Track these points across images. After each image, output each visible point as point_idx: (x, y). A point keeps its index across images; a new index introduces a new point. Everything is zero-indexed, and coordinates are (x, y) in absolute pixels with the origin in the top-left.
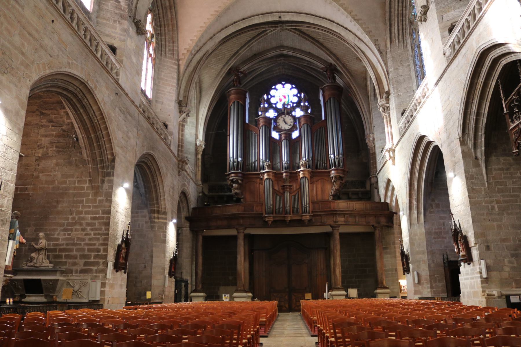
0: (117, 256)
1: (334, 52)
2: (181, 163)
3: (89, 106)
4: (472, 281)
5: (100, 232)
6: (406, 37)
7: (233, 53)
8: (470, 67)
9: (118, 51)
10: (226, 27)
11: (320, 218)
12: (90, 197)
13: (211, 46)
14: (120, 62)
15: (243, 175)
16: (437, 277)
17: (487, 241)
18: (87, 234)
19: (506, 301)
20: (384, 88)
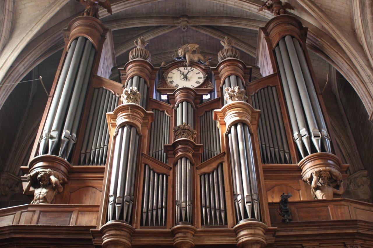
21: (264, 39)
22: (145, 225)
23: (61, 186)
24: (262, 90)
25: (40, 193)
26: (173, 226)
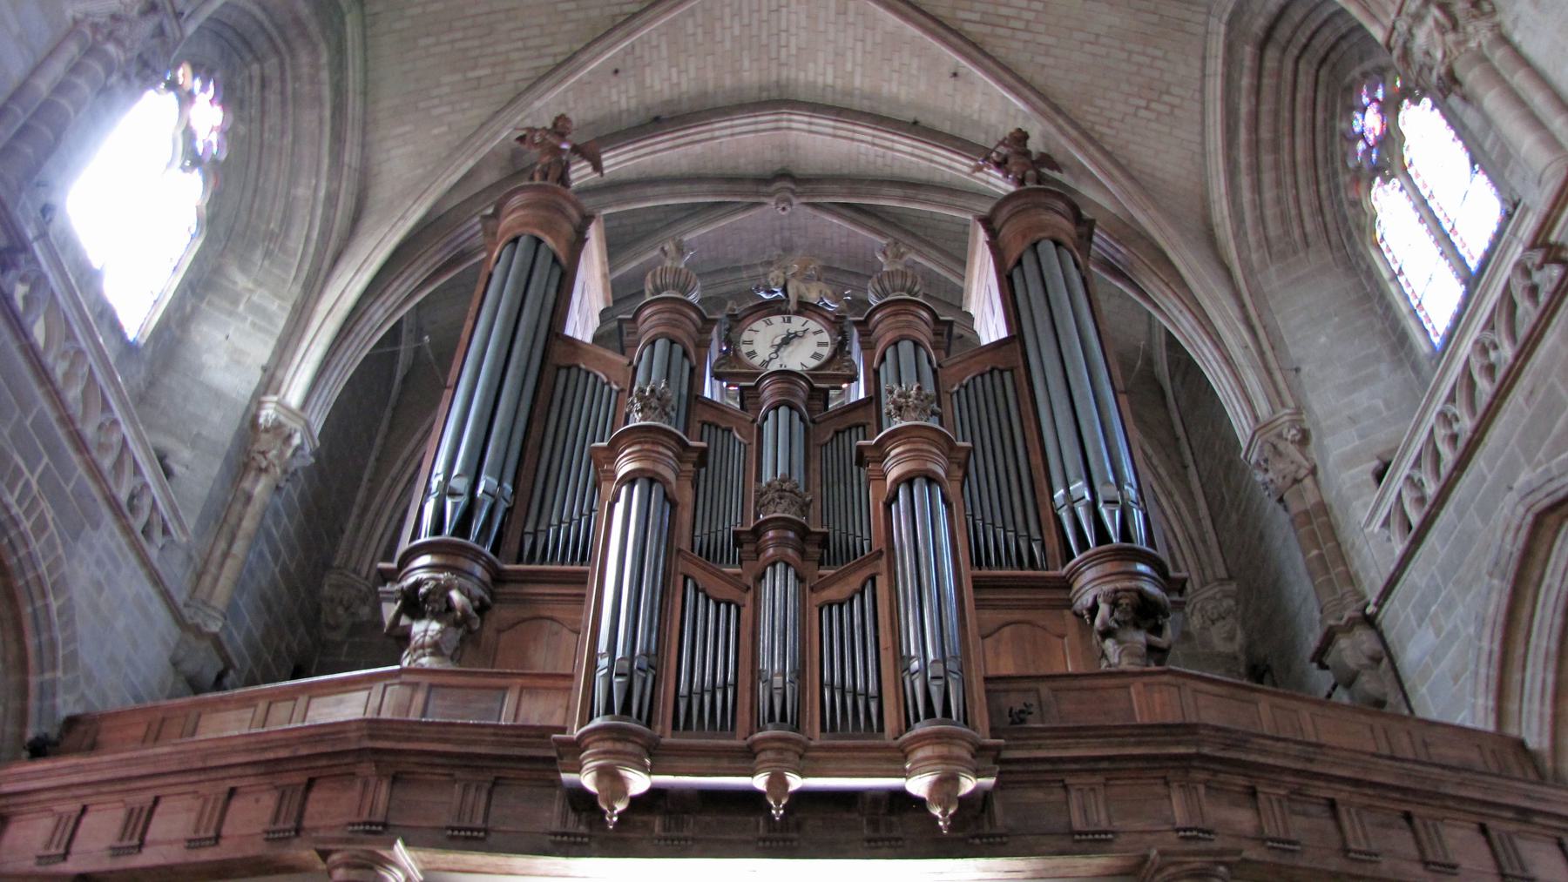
1: (1039, 80)
7: (549, 61)
11: (1057, 795)
15: (498, 577)
21: (987, 247)
22: (685, 729)
23: (475, 615)
24: (979, 379)
25: (426, 631)
26: (751, 733)
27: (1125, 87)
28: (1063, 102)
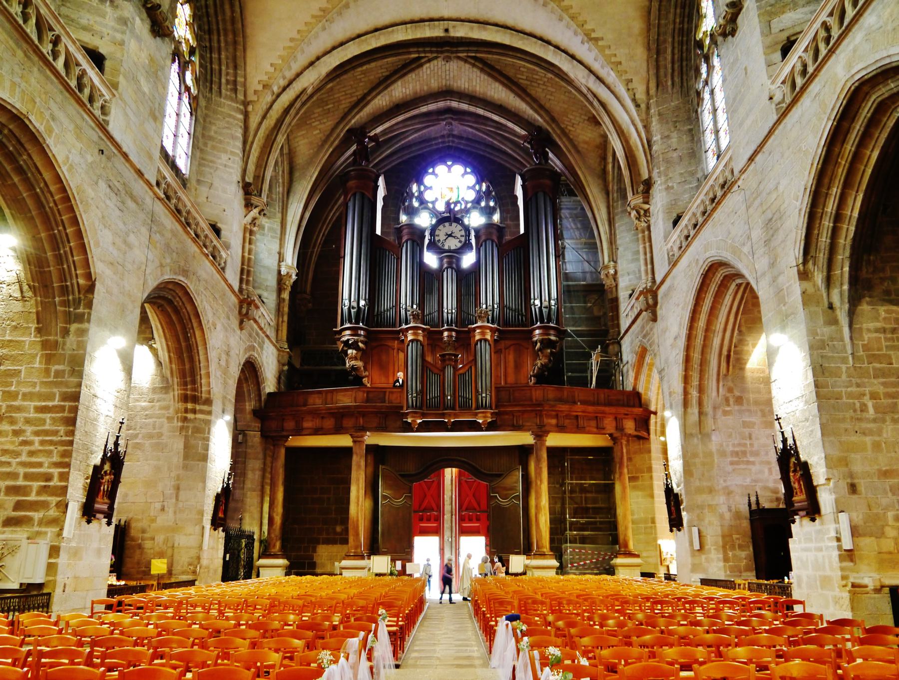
0: (93, 491)
1: (547, 106)
2: (245, 306)
3: (34, 170)
4: (820, 554)
5: (54, 438)
6: (687, 75)
7: (355, 99)
8: (829, 119)
9: (108, 64)
10: (342, 44)
12: (37, 365)
13: (312, 80)
14: (113, 86)
16: (737, 539)
17: (851, 475)
18: (25, 443)
19: (889, 599)
20: (639, 175)
27: (580, 111)
28: (556, 115)
